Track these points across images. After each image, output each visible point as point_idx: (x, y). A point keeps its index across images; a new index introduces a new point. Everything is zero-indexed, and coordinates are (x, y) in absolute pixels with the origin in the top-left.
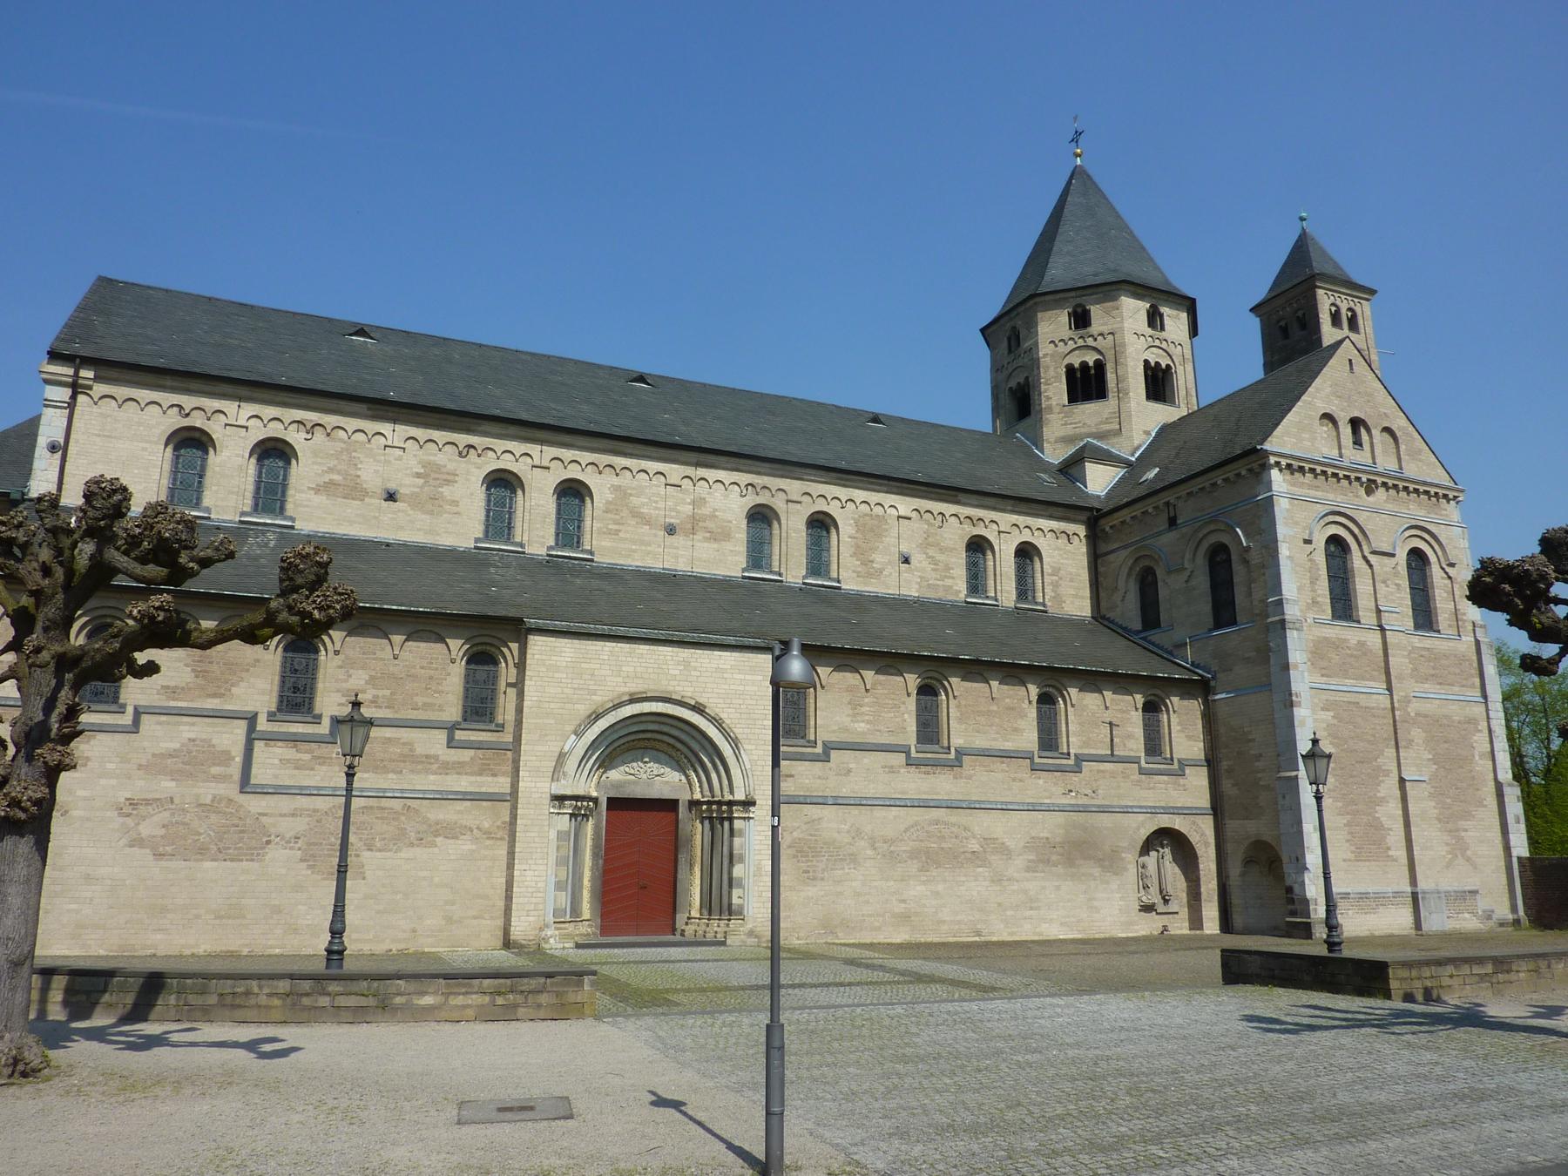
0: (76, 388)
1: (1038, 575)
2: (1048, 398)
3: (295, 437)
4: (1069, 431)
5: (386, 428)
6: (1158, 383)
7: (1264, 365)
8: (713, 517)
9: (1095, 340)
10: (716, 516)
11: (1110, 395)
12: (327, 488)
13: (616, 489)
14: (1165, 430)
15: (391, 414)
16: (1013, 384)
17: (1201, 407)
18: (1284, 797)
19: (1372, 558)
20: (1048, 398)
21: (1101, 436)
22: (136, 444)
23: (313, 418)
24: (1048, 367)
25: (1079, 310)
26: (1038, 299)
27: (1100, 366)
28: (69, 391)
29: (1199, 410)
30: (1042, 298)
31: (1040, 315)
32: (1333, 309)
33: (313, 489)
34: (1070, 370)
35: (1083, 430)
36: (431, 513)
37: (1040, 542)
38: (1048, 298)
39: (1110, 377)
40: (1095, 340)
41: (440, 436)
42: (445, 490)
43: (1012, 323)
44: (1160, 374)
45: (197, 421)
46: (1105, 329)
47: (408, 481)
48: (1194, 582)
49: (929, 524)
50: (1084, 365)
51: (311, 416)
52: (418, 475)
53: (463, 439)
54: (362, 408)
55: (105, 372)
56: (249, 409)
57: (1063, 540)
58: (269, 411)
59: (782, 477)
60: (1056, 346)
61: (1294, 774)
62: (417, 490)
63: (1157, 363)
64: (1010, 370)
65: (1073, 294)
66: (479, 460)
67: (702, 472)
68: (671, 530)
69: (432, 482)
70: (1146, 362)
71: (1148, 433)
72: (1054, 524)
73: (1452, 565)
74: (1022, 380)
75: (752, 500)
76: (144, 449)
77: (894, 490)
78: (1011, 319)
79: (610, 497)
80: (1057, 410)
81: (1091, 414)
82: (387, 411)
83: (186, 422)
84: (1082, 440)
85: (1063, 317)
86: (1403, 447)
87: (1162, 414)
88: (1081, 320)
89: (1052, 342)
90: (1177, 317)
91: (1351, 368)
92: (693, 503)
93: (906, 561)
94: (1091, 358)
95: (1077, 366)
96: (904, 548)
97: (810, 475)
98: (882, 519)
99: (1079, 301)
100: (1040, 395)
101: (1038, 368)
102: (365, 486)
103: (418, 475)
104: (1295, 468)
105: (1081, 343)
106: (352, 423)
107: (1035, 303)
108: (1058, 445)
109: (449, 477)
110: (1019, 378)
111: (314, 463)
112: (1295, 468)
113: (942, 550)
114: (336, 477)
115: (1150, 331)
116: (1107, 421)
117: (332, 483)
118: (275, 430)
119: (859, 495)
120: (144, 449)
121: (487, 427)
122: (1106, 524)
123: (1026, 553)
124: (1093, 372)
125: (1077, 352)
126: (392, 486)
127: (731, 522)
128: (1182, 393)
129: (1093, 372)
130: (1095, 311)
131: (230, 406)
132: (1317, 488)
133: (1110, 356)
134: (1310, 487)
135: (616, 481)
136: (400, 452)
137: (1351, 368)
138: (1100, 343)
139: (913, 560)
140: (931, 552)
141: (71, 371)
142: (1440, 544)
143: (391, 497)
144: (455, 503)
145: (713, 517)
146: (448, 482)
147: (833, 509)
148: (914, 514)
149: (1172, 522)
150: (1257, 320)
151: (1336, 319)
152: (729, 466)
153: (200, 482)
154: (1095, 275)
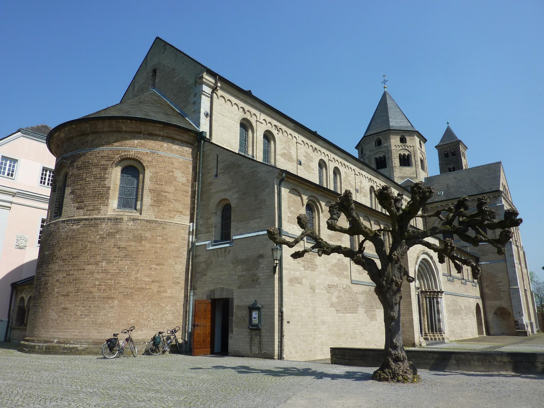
0: (214, 90)
2: (395, 163)
3: (275, 132)
4: (401, 175)
5: (296, 135)
7: (439, 164)
9: (408, 147)
10: (364, 188)
11: (413, 166)
12: (283, 155)
15: (298, 130)
16: (377, 156)
18: (513, 294)
20: (395, 163)
22: (232, 121)
23: (280, 126)
24: (394, 153)
25: (402, 137)
26: (391, 131)
27: (409, 156)
28: (211, 90)
30: (392, 131)
31: (391, 136)
33: (280, 155)
34: (400, 155)
35: (406, 175)
36: (308, 172)
38: (394, 131)
40: (408, 147)
43: (378, 137)
45: (248, 116)
46: (411, 145)
50: (404, 154)
53: (315, 146)
54: (292, 125)
55: (225, 87)
56: (263, 116)
58: (269, 119)
59: (376, 177)
60: (396, 147)
61: (517, 287)
62: (305, 162)
64: (376, 152)
65: (401, 132)
66: (317, 154)
67: (362, 172)
69: (308, 160)
74: (382, 156)
76: (234, 124)
77: (394, 187)
78: (377, 136)
80: (397, 168)
81: (407, 171)
82: (298, 128)
84: (406, 178)
85: (398, 139)
88: (403, 140)
89: (395, 145)
94: (407, 153)
95: (402, 155)
97: (381, 178)
99: (402, 134)
100: (392, 162)
101: (391, 153)
102: (293, 157)
103: (304, 156)
105: (404, 147)
106: (290, 131)
107: (390, 132)
109: (312, 159)
111: (280, 144)
114: (286, 152)
116: (412, 174)
117: (284, 153)
118: (269, 127)
120: (234, 124)
121: (321, 142)
125: (402, 150)
127: (367, 191)
129: (406, 157)
130: (408, 138)
131: (258, 113)
133: (413, 153)
138: (409, 149)
141: (213, 81)
143: (300, 164)
144: (313, 170)
146: (312, 161)
150: (437, 150)
152: (367, 171)
153: (245, 144)
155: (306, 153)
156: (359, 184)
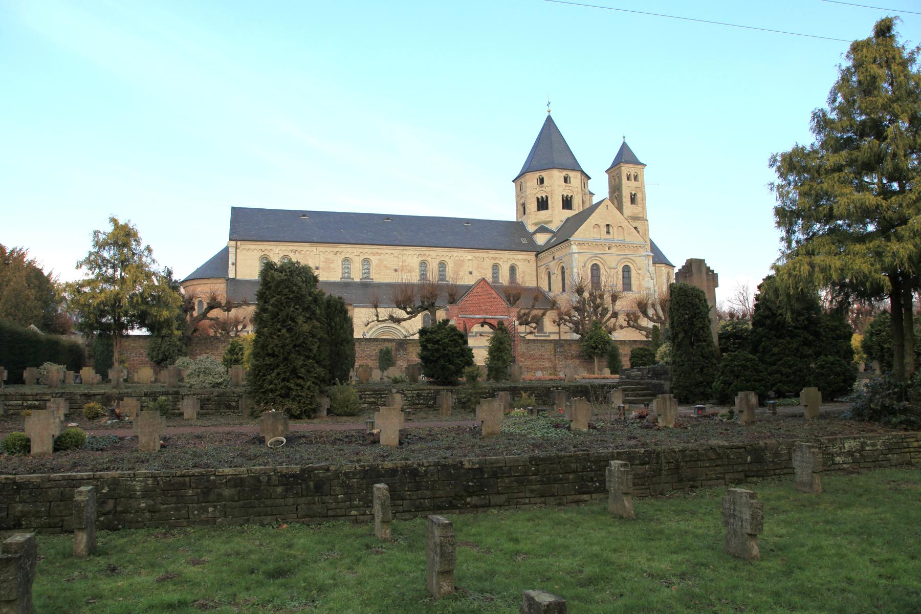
1: (517, 274)
2: (530, 209)
4: (536, 221)
5: (314, 249)
6: (567, 203)
8: (409, 265)
11: (549, 208)
13: (379, 260)
14: (568, 219)
17: (585, 208)
19: (607, 270)
21: (547, 223)
27: (547, 197)
29: (583, 210)
32: (629, 174)
34: (538, 198)
37: (518, 263)
39: (549, 202)
41: (328, 249)
42: (331, 265)
44: (569, 199)
47: (321, 264)
48: (558, 277)
49: (478, 261)
51: (295, 248)
52: (324, 262)
55: (243, 242)
57: (526, 263)
58: (284, 248)
63: (567, 195)
68: (396, 270)
70: (563, 195)
71: (562, 221)
72: (523, 257)
73: (640, 269)
75: (420, 259)
79: (377, 262)
81: (543, 215)
83: (264, 253)
86: (625, 232)
87: (569, 213)
90: (576, 177)
91: (607, 209)
92: (402, 262)
93: (471, 273)
96: (470, 270)
98: (463, 261)
103: (324, 262)
104: (580, 244)
106: (305, 249)
108: (533, 226)
110: (522, 201)
112: (580, 244)
113: (483, 269)
115: (565, 184)
116: (548, 218)
119: (455, 254)
122: (540, 256)
123: (513, 269)
124: (545, 199)
126: (317, 265)
128: (577, 205)
132: (589, 249)
134: (587, 249)
135: (379, 257)
136: (318, 256)
137: (607, 209)
138: (548, 189)
139: (473, 273)
140: (480, 270)
142: (636, 263)
144: (334, 268)
145: (409, 265)
146: (332, 263)
147: (447, 259)
148: (474, 259)
149: (554, 258)
151: (628, 179)
154: (546, 165)
155: (326, 258)
156: (401, 264)
